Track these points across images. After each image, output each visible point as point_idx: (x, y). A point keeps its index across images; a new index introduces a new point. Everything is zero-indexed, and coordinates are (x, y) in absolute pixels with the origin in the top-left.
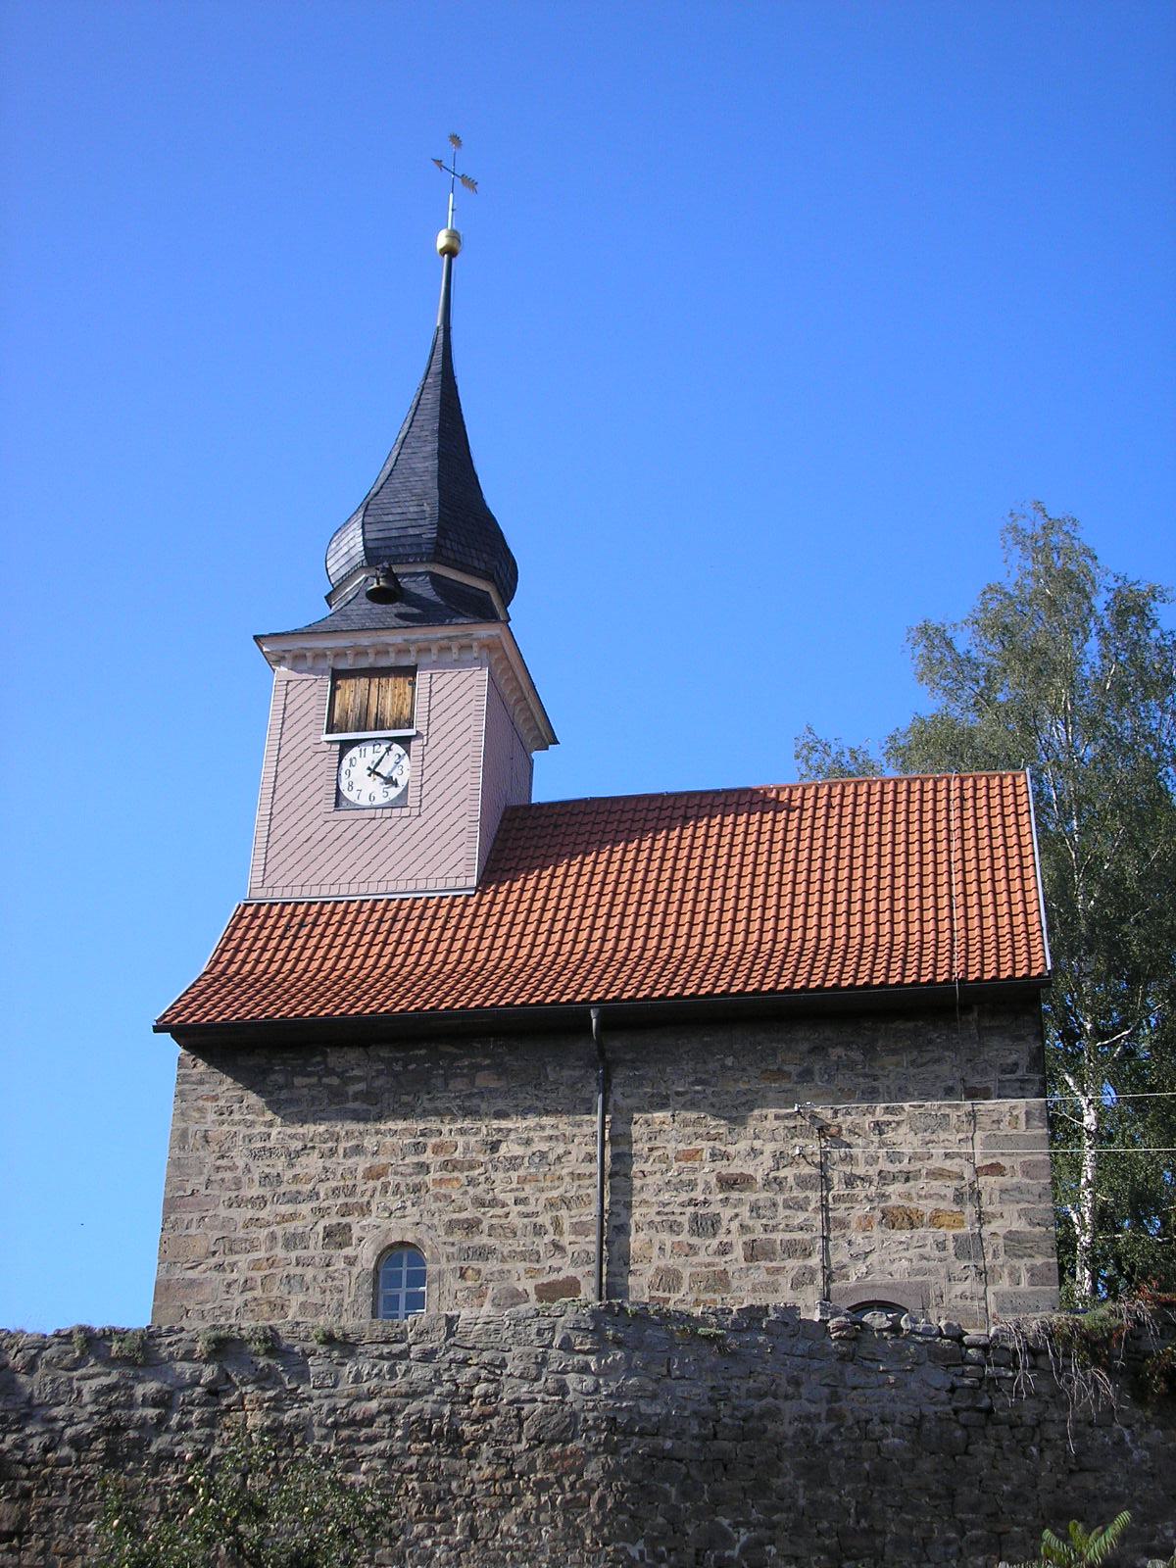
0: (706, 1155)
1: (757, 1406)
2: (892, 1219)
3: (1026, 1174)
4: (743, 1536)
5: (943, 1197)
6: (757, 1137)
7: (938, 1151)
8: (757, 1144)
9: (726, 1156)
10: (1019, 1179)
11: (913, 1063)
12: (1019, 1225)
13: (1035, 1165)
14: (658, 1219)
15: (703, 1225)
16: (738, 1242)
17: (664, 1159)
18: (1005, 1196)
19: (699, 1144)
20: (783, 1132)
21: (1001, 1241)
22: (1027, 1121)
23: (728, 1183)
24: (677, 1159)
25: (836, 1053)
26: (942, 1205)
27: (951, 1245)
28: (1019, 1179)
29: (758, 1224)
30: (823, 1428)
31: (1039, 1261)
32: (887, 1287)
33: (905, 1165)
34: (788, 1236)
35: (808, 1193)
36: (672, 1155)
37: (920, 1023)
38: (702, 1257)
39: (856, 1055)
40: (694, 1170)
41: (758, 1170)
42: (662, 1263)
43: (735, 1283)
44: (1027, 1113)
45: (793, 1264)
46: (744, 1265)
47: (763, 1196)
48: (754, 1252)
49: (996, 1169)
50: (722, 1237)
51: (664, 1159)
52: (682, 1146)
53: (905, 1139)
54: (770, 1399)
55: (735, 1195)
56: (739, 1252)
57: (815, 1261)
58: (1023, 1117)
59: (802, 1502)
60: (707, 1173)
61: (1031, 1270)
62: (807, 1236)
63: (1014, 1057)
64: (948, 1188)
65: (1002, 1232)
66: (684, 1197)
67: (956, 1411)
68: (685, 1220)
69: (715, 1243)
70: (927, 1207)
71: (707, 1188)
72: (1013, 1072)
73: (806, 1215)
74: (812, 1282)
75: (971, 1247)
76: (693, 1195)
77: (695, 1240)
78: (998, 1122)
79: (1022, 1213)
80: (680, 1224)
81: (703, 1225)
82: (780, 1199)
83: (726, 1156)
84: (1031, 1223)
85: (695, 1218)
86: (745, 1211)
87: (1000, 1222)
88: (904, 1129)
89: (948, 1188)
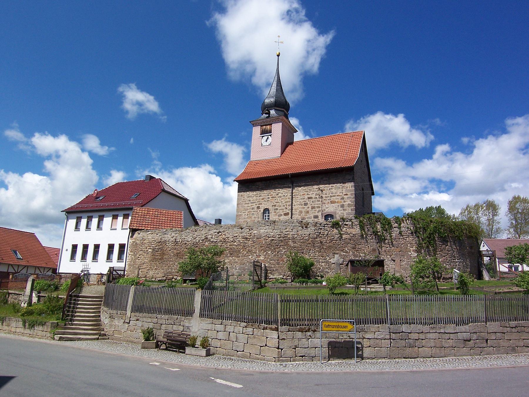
0: (306, 194)
1: (287, 233)
2: (332, 202)
3: (351, 195)
4: (284, 250)
5: (339, 199)
6: (313, 191)
7: (339, 192)
8: (313, 192)
9: (309, 194)
10: (350, 196)
11: (335, 179)
12: (350, 203)
13: (353, 194)
14: (299, 204)
15: (306, 204)
16: (310, 206)
17: (300, 195)
18: (348, 198)
19: (305, 193)
20: (317, 191)
21: (347, 205)
22: (352, 187)
23: (309, 198)
24: (302, 195)
25: (324, 179)
26: (339, 200)
27: (340, 206)
28: (350, 196)
29: (313, 204)
30: (296, 236)
31: (352, 208)
32: (331, 212)
33: (334, 195)
34: (317, 205)
35: (320, 199)
36: (301, 195)
37: (336, 173)
38: (305, 209)
39: (327, 179)
40: (304, 197)
41: (313, 196)
42: (300, 210)
43: (309, 212)
44: (352, 186)
45: (318, 209)
46: (311, 210)
47: (314, 200)
48: (313, 208)
49: (346, 195)
50: (308, 206)
51: (300, 195)
52: (303, 193)
53: (334, 190)
54: (288, 232)
55: (310, 200)
56: (310, 208)
57: (321, 209)
58: (351, 187)
59: (292, 246)
60: (306, 197)
61: (351, 209)
62: (320, 205)
63: (350, 178)
64: (340, 198)
65: (347, 204)
66: (303, 200)
67: (315, 233)
68: (303, 204)
69: (307, 207)
70: (337, 200)
71: (306, 199)
72: (349, 180)
73: (320, 202)
74: (320, 211)
75: (342, 206)
76: (304, 200)
77: (305, 206)
78: (347, 188)
79: (350, 201)
80: (302, 204)
81: (306, 204)
82: (316, 200)
83: (309, 194)
84: (351, 202)
85: (304, 203)
86: (311, 202)
87: (347, 202)
88: (334, 189)
89: (340, 198)
